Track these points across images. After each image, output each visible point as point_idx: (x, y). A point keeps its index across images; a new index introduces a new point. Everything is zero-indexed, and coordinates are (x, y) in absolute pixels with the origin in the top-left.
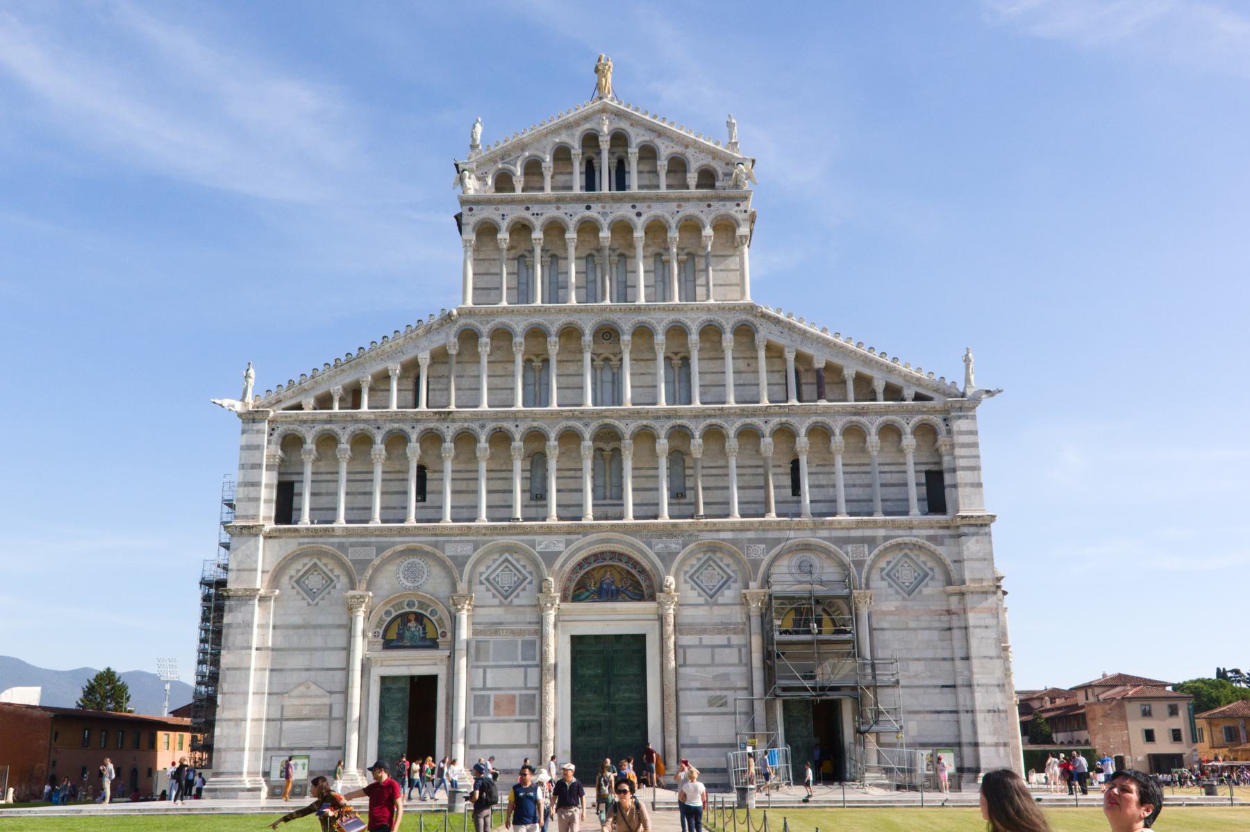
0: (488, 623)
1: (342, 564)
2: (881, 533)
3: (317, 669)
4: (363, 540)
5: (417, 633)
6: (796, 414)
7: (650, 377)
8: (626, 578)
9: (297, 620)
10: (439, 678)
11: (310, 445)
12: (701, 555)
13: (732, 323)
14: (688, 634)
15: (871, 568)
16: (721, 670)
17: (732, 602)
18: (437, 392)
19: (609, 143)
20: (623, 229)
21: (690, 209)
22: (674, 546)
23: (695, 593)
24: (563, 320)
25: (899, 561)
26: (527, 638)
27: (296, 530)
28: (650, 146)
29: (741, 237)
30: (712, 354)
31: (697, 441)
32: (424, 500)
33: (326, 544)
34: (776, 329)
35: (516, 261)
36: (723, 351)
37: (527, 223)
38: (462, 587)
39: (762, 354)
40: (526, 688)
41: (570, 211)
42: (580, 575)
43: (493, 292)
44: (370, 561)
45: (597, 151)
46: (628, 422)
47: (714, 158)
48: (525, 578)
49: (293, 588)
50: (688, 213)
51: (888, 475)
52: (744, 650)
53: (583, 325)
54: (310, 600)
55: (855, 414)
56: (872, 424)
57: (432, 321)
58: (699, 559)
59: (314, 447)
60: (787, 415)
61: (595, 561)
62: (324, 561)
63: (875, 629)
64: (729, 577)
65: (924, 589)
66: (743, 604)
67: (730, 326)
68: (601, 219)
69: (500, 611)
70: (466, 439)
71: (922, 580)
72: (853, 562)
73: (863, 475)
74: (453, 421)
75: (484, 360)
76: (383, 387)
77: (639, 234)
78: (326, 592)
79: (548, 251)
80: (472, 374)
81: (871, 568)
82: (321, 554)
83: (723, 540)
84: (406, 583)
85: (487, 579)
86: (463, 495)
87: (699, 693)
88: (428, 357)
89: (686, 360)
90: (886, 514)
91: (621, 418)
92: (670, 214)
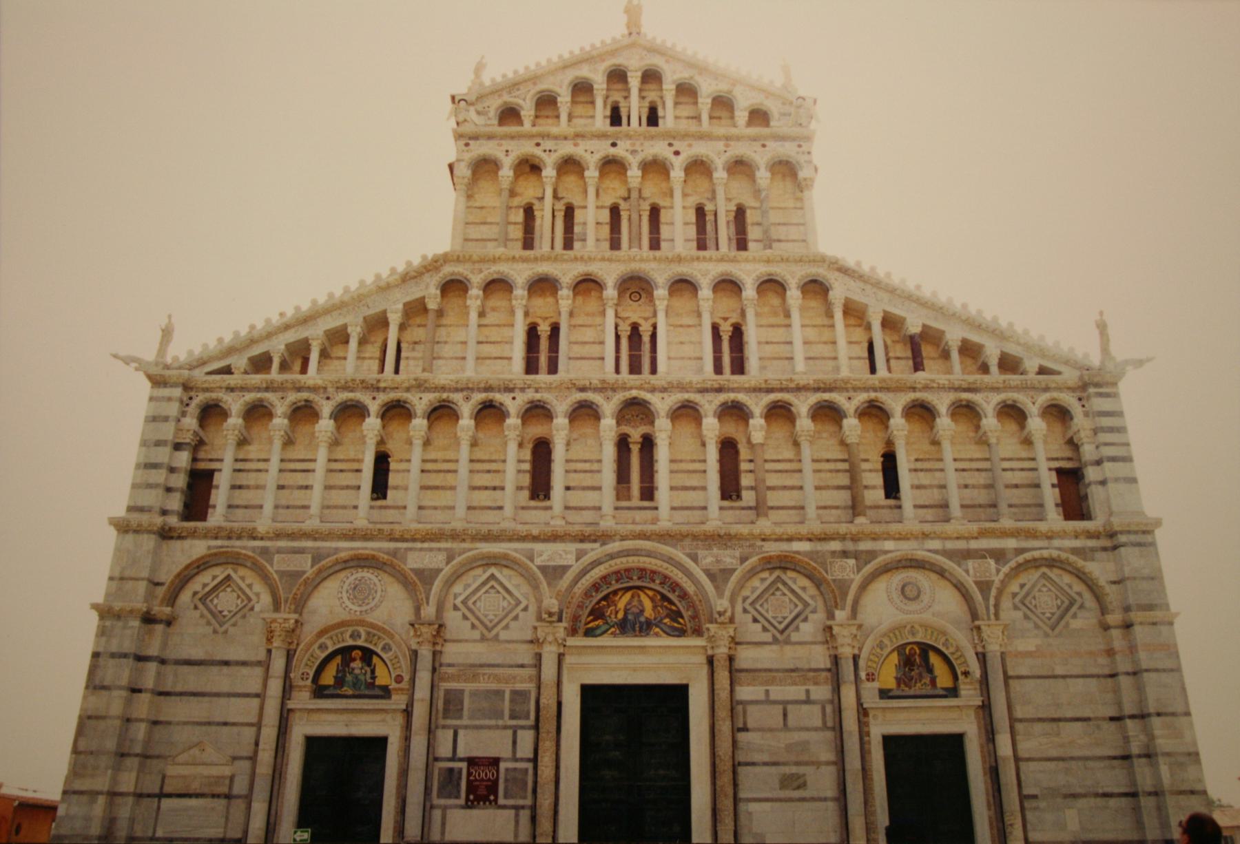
0: (463, 665)
2: (1011, 543)
3: (218, 724)
4: (296, 544)
5: (362, 677)
8: (662, 606)
9: (197, 653)
10: (390, 740)
11: (235, 421)
12: (765, 575)
14: (749, 685)
15: (1000, 592)
16: (797, 737)
17: (808, 638)
18: (412, 362)
20: (656, 168)
22: (728, 560)
23: (758, 627)
26: (519, 686)
28: (689, 84)
29: (805, 179)
30: (773, 320)
31: (757, 422)
32: (385, 497)
33: (244, 548)
34: (852, 284)
37: (536, 162)
38: (429, 611)
40: (515, 760)
42: (595, 601)
43: (490, 245)
44: (304, 572)
45: (626, 94)
46: (665, 395)
47: (767, 98)
49: (196, 608)
51: (1009, 474)
52: (829, 709)
53: (605, 276)
54: (217, 626)
56: (988, 403)
58: (763, 580)
59: (240, 421)
61: (617, 581)
62: (242, 571)
63: (1011, 677)
64: (806, 605)
65: (1072, 621)
66: (827, 642)
67: (796, 280)
68: (629, 157)
69: (480, 648)
71: (1067, 610)
73: (976, 473)
74: (428, 390)
75: (473, 316)
76: (341, 354)
77: (677, 174)
78: (239, 615)
79: (562, 198)
81: (1000, 592)
83: (798, 553)
84: (351, 606)
85: (464, 602)
86: (437, 492)
87: (766, 769)
89: (737, 332)
91: (653, 390)
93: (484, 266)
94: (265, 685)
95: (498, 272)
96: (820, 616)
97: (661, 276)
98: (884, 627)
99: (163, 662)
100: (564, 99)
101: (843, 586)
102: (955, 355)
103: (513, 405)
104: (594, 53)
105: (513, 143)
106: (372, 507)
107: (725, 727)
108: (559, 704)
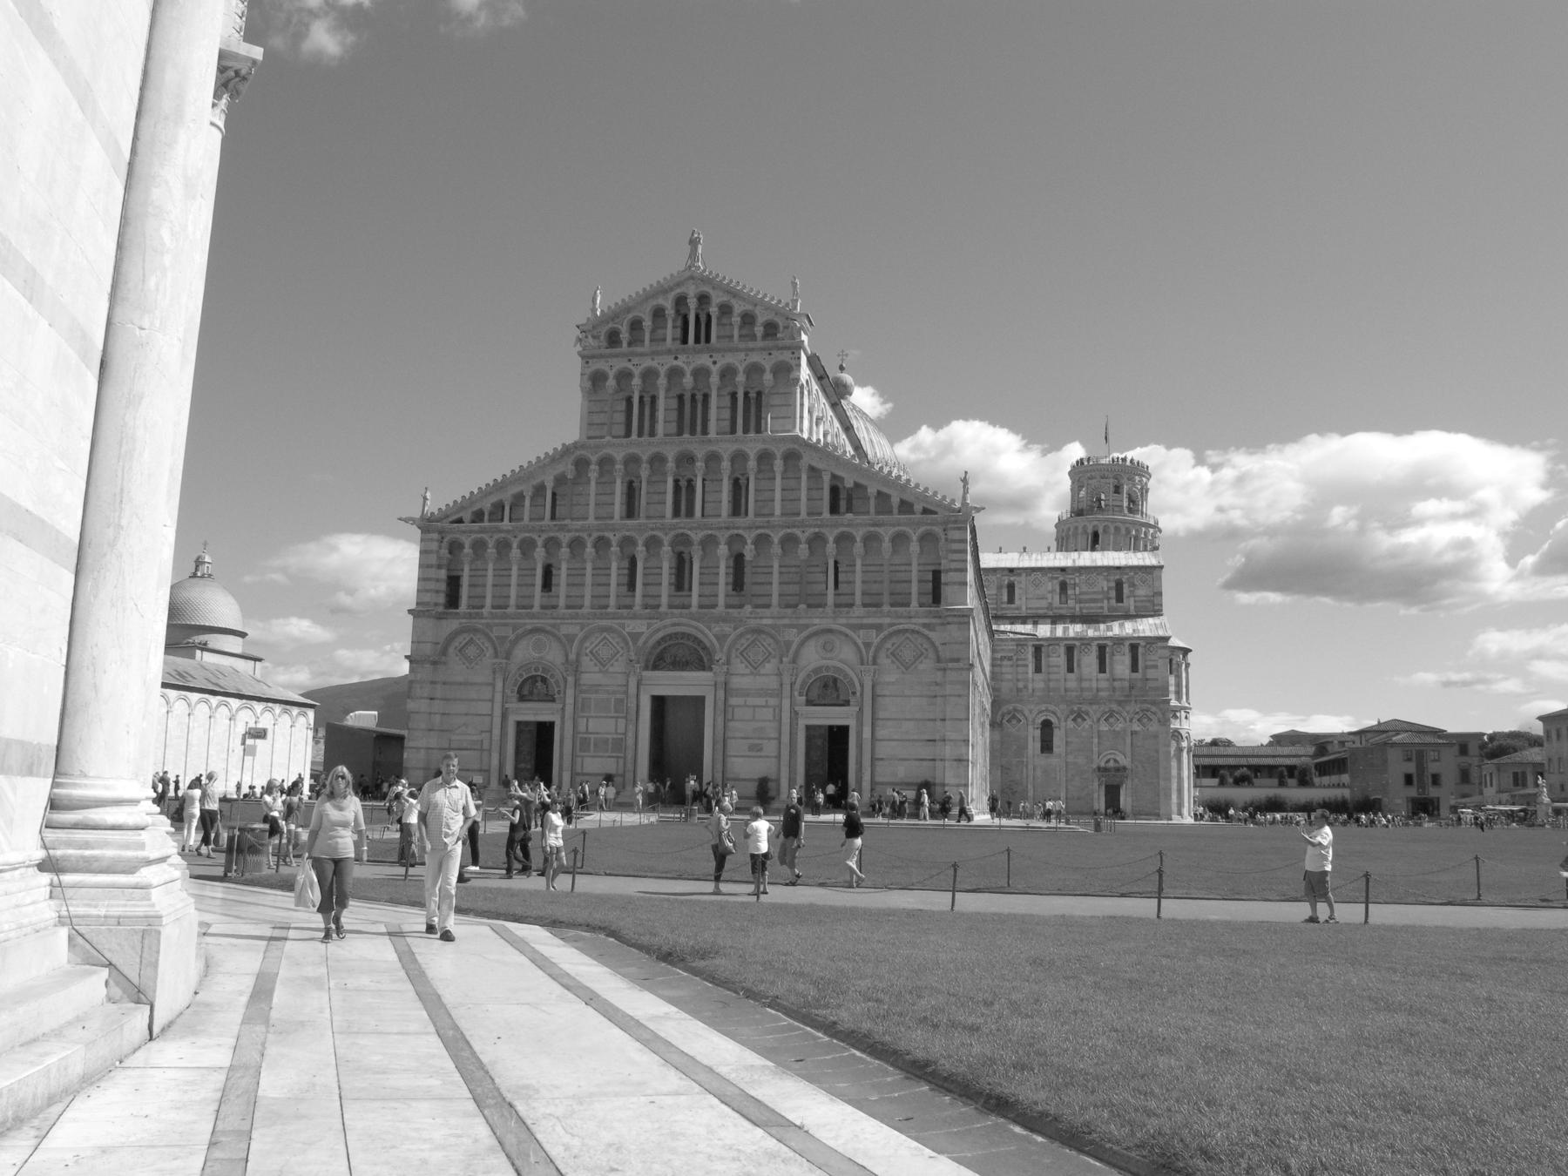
1: (490, 639)
2: (887, 620)
6: (827, 526)
9: (460, 679)
11: (467, 550)
12: (749, 636)
20: (701, 373)
21: (755, 358)
23: (743, 665)
24: (654, 450)
25: (901, 644)
26: (618, 696)
27: (457, 613)
32: (550, 590)
35: (624, 403)
38: (572, 657)
39: (804, 477)
40: (617, 733)
42: (658, 651)
48: (618, 652)
50: (755, 360)
52: (777, 711)
55: (873, 525)
59: (471, 551)
60: (819, 526)
64: (770, 654)
68: (686, 368)
70: (576, 545)
72: (864, 643)
74: (569, 531)
75: (593, 483)
77: (715, 379)
82: (476, 630)
85: (591, 652)
90: (892, 605)
91: (690, 529)
92: (739, 361)
94: (493, 696)
96: (774, 661)
97: (700, 453)
98: (811, 667)
99: (444, 683)
100: (647, 324)
101: (788, 644)
102: (872, 502)
103: (614, 539)
104: (666, 286)
105: (615, 360)
106: (542, 597)
107: (720, 720)
108: (638, 706)
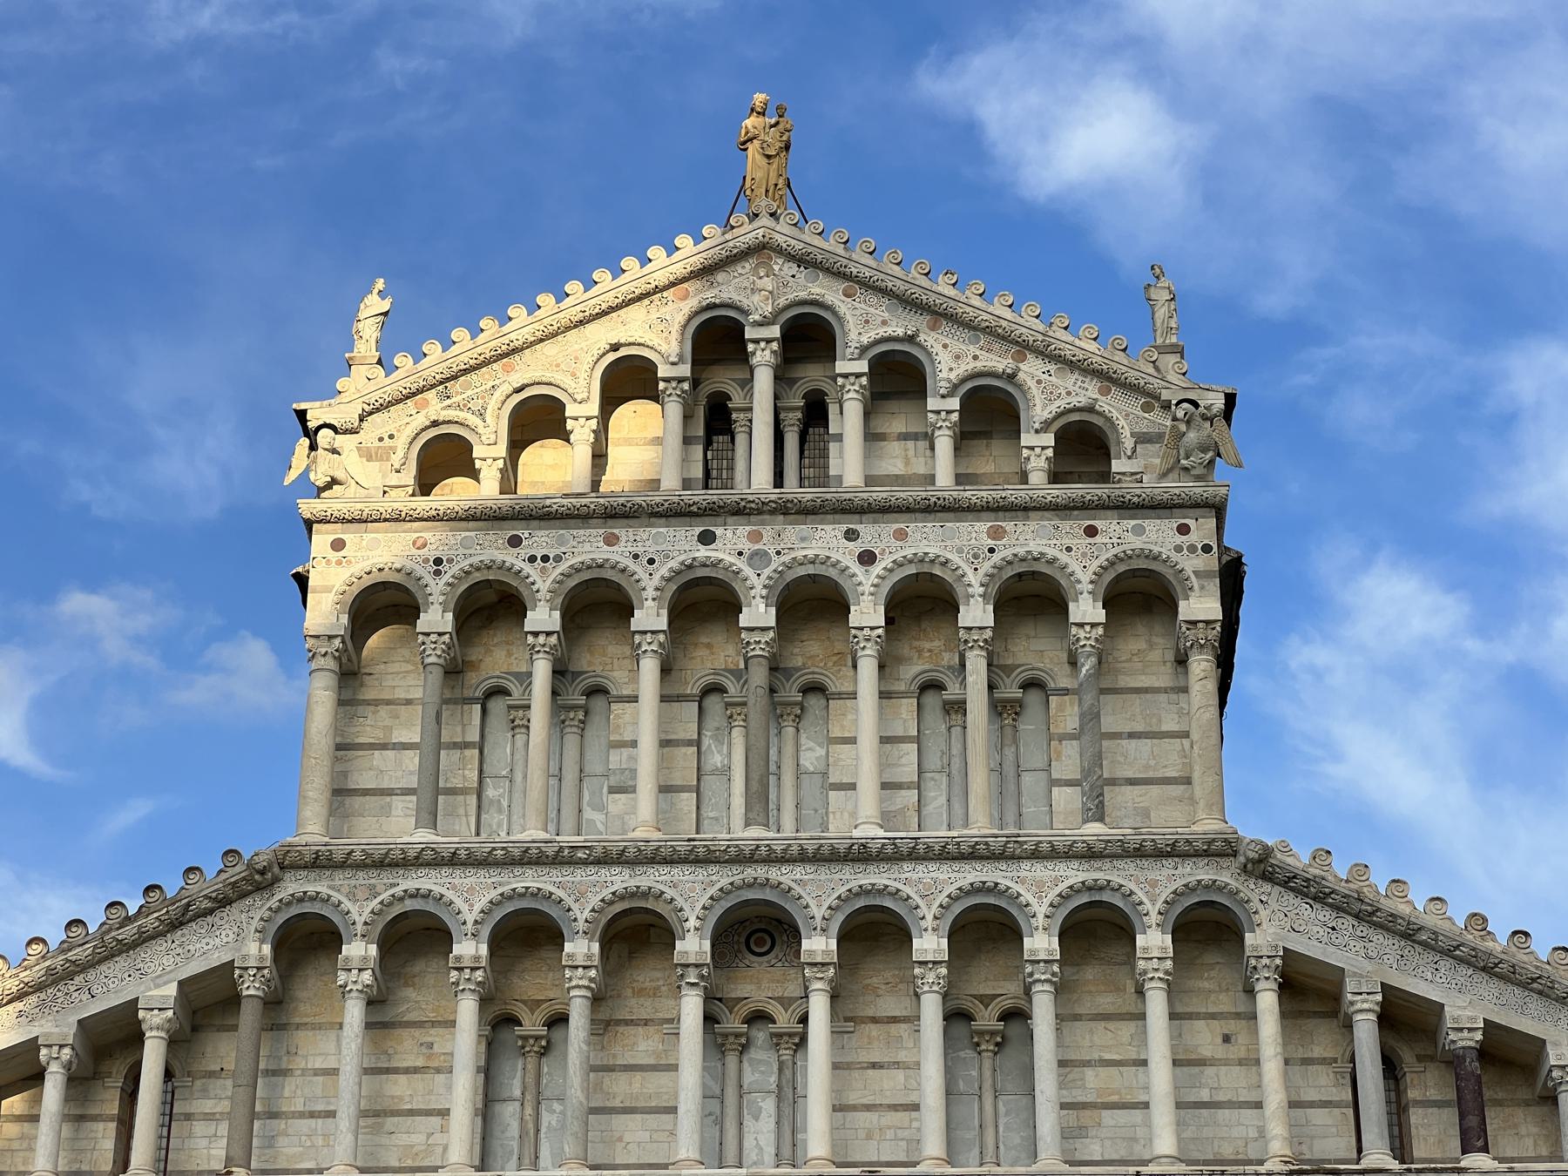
7: (900, 1075)
13: (1166, 894)
19: (775, 346)
24: (619, 880)
34: (1313, 917)
36: (1140, 992)
39: (1267, 1001)
41: (651, 550)
47: (1105, 392)
50: (1021, 551)
53: (680, 902)
57: (193, 889)
67: (1159, 905)
68: (748, 571)
80: (319, 1063)
88: (171, 1003)
93: (386, 877)
95: (416, 894)
